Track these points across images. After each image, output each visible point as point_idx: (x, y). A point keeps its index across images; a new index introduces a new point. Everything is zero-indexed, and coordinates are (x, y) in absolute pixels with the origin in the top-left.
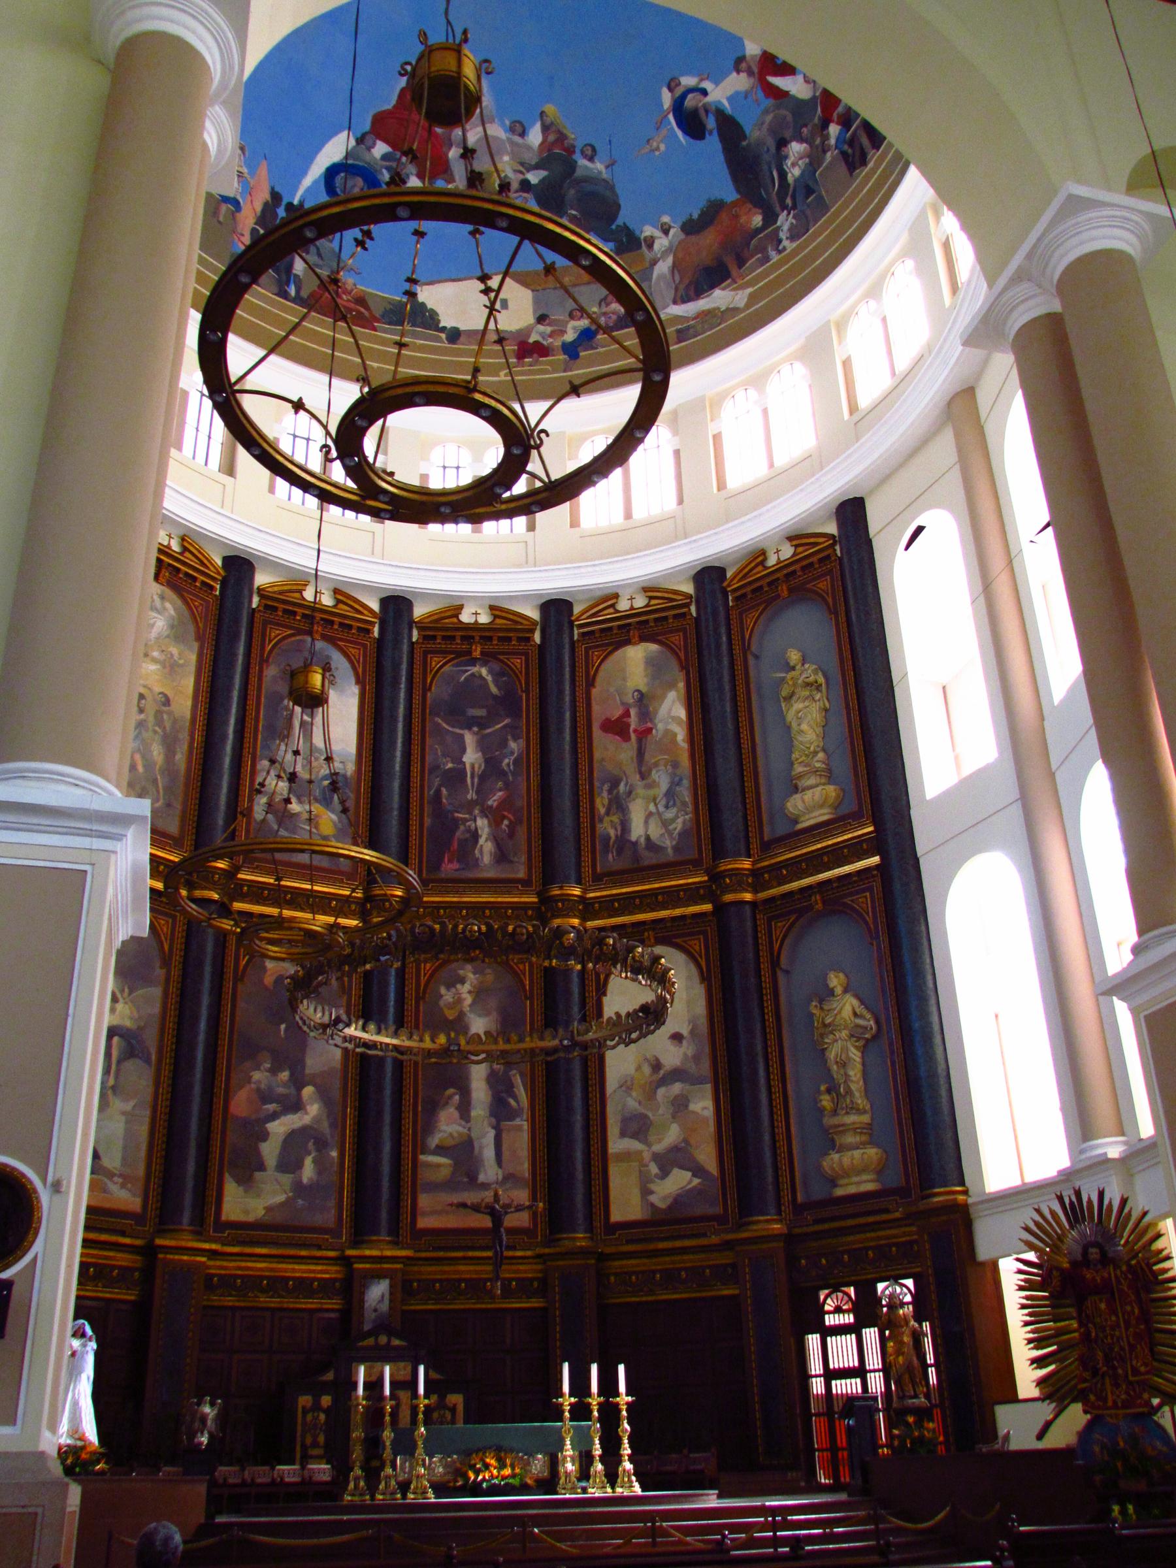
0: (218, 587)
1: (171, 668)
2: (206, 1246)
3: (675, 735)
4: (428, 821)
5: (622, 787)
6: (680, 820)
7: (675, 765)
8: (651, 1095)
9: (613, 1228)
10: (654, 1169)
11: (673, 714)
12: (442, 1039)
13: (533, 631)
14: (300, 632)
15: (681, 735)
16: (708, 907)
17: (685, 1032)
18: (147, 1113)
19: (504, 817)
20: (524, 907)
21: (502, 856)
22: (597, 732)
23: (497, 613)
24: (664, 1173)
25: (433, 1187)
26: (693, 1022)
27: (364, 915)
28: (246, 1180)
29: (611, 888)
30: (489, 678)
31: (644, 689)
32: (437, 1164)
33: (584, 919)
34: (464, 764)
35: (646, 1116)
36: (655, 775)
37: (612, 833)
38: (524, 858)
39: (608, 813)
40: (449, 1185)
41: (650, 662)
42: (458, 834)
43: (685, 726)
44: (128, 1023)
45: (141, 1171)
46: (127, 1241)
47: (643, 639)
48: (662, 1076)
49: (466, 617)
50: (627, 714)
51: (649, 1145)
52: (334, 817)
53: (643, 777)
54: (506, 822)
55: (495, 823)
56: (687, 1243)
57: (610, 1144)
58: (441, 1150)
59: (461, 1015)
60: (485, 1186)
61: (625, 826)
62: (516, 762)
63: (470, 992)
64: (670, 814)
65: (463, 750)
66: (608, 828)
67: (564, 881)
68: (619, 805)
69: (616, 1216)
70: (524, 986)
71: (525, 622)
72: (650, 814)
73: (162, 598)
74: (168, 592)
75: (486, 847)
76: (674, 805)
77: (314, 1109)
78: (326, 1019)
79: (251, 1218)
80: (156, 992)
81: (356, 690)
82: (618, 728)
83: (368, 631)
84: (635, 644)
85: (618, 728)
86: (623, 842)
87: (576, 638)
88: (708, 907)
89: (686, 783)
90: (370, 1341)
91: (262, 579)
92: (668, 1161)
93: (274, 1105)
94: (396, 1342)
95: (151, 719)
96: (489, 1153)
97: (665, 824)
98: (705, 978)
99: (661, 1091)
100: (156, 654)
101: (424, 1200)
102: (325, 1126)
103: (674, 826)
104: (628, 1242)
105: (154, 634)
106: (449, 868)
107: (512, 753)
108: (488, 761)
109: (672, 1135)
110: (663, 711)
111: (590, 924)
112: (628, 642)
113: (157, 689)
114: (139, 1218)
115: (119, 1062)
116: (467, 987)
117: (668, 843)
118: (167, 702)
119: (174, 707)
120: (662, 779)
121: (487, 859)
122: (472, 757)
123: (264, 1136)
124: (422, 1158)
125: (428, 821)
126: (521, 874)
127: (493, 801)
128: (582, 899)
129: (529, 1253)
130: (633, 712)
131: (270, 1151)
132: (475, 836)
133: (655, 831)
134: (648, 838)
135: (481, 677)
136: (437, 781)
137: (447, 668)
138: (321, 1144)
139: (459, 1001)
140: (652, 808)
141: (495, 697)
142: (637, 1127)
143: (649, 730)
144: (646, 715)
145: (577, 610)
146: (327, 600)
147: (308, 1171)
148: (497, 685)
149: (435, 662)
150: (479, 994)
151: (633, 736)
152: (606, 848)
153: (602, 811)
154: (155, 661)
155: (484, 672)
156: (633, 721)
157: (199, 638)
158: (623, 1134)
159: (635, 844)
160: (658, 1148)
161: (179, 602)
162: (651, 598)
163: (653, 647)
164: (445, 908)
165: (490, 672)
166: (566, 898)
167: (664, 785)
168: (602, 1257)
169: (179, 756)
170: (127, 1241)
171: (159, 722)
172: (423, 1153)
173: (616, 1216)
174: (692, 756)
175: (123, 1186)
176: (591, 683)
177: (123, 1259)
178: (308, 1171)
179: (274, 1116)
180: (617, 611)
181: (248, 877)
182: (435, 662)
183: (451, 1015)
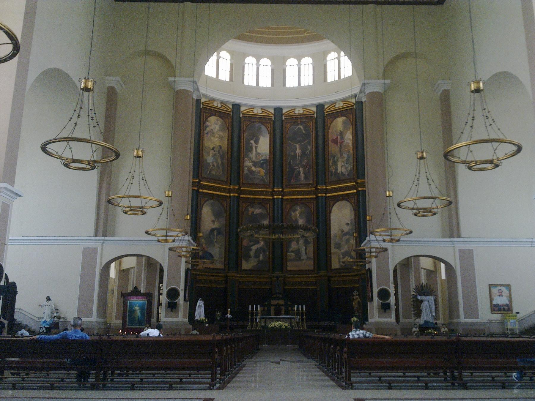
0: (231, 113)
1: (221, 138)
2: (238, 275)
3: (349, 143)
4: (287, 170)
5: (336, 158)
6: (350, 167)
7: (349, 152)
8: (341, 238)
9: (332, 270)
10: (341, 256)
11: (349, 137)
12: (277, 236)
13: (313, 114)
14: (253, 122)
15: (351, 144)
16: (355, 191)
17: (349, 223)
19: (306, 167)
20: (312, 191)
21: (306, 178)
22: (330, 142)
23: (304, 110)
24: (344, 257)
25: (291, 260)
26: (351, 220)
29: (332, 186)
30: (303, 129)
31: (342, 130)
32: (291, 255)
33: (326, 194)
34: (296, 153)
35: (340, 243)
36: (344, 155)
37: (333, 170)
38: (312, 178)
39: (332, 165)
41: (344, 122)
42: (295, 172)
43: (352, 141)
44: (218, 227)
46: (221, 275)
47: (342, 116)
48: (344, 234)
49: (297, 112)
50: (337, 138)
51: (340, 250)
52: (264, 170)
53: (341, 155)
54: (307, 168)
55: (304, 169)
56: (348, 274)
57: (332, 250)
58: (292, 252)
59: (297, 218)
60: (303, 260)
61: (336, 169)
63: (298, 213)
64: (347, 166)
65: (296, 150)
66: (332, 169)
68: (335, 163)
69: (333, 267)
70: (311, 210)
71: (312, 112)
72: (343, 166)
73: (217, 120)
74: (219, 118)
75: (302, 175)
76: (348, 163)
77: (262, 243)
78: (250, 234)
79: (248, 269)
80: (223, 219)
81: (268, 136)
82: (335, 141)
83: (271, 119)
84: (340, 117)
85: (335, 141)
86: (336, 173)
87: (325, 115)
88: (355, 191)
89: (351, 157)
90: (275, 296)
91: (242, 109)
92: (345, 254)
93: (252, 243)
94: (281, 296)
96: (304, 252)
97: (346, 168)
98: (354, 209)
99: (344, 237)
100: (217, 136)
103: (348, 169)
104: (335, 273)
105: (216, 129)
106: (293, 181)
107: (309, 149)
108: (302, 152)
109: (345, 248)
110: (346, 137)
111: (327, 195)
112: (338, 117)
113: (218, 144)
114: (224, 270)
115: (217, 236)
116: (298, 212)
117: (346, 173)
118: (221, 147)
119: (223, 148)
120: (345, 156)
121: (302, 179)
122: (298, 151)
123: (251, 250)
124: (288, 254)
125: (287, 170)
126: (311, 182)
127: (304, 163)
128: (326, 188)
129: (312, 276)
130: (339, 137)
131: (252, 253)
132: (299, 172)
133: (344, 170)
134: (342, 172)
135: (301, 129)
136: (290, 158)
137: (292, 127)
138: (264, 251)
139: (296, 215)
140: (343, 164)
142: (338, 246)
143: (343, 142)
144: (342, 138)
145: (326, 107)
146: (260, 112)
147: (261, 257)
148: (304, 131)
149: (288, 125)
150: (301, 213)
151: (339, 144)
152: (332, 175)
153: (331, 165)
154: (217, 137)
155: (301, 127)
156: (339, 139)
157: (228, 129)
158: (335, 248)
159: (339, 174)
160: (343, 251)
162: (344, 104)
163: (344, 118)
164: (292, 192)
167: (346, 158)
168: (329, 277)
170: (221, 275)
171: (219, 152)
172: (288, 252)
173: (333, 267)
174: (353, 149)
175: (219, 263)
176: (329, 129)
177: (221, 279)
178: (261, 257)
179: (253, 245)
180: (336, 108)
181: (244, 189)
182: (288, 125)
183: (294, 219)
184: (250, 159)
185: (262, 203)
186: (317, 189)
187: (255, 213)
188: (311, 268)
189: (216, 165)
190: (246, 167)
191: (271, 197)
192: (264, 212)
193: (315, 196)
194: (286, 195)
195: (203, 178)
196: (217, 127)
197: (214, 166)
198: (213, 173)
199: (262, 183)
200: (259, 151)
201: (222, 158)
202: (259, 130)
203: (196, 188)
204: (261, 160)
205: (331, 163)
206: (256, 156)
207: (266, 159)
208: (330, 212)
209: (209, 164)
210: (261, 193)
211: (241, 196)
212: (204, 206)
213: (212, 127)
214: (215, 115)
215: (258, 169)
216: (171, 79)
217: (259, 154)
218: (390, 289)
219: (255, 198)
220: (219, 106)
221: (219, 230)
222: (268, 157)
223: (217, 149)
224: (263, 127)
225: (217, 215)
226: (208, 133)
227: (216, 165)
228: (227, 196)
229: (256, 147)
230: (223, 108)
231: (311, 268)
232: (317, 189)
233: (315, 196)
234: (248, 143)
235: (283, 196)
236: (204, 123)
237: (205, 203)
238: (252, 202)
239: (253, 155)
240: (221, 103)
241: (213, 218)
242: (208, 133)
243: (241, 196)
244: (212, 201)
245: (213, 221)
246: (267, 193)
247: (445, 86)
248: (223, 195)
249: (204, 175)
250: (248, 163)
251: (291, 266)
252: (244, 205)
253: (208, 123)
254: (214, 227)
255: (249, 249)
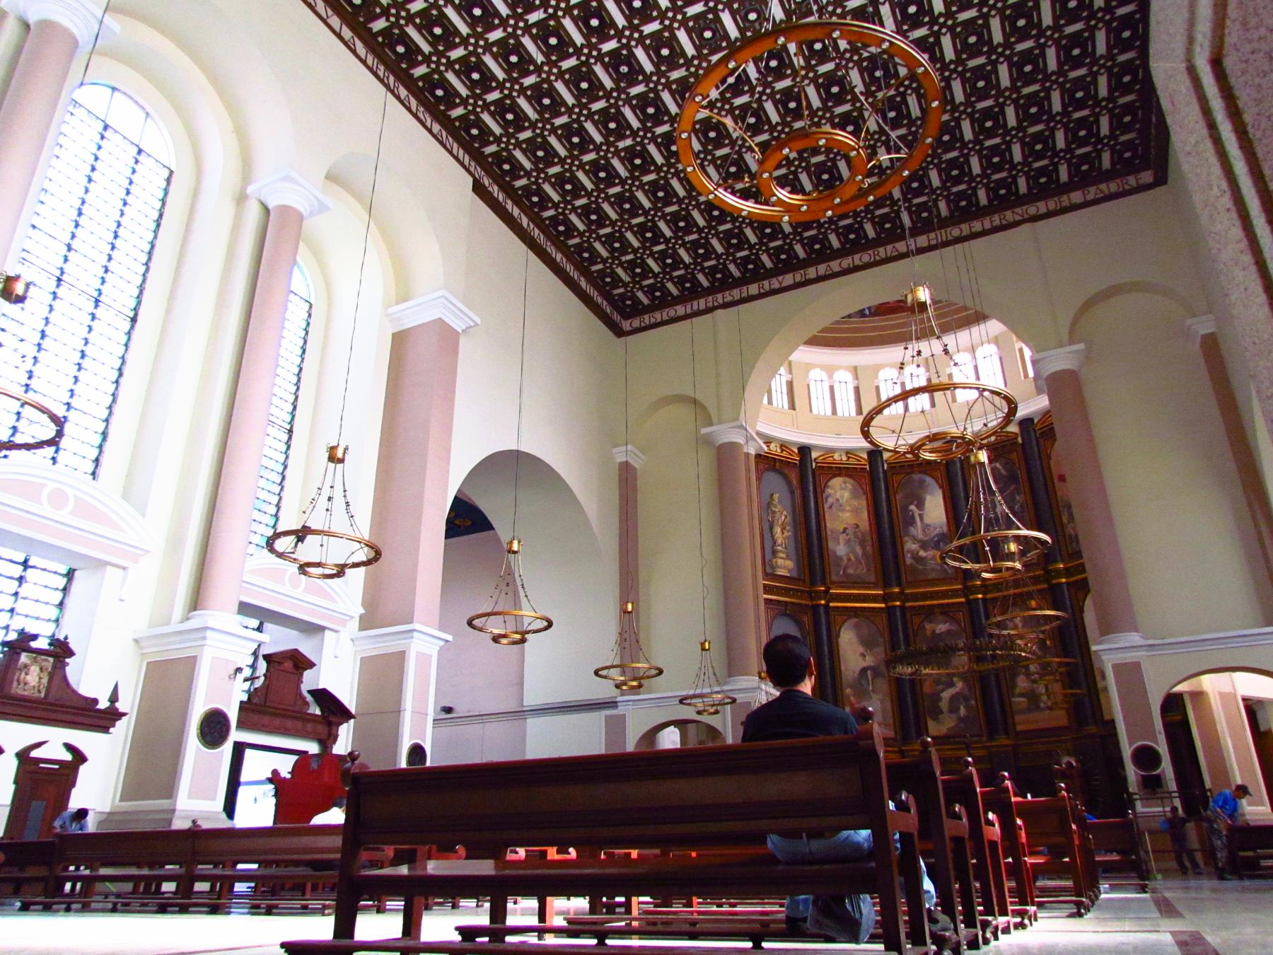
1: (855, 511)
13: (1016, 438)
14: (908, 474)
18: (888, 699)
20: (1039, 576)
25: (1020, 712)
27: (966, 596)
28: (935, 718)
32: (1020, 702)
39: (1069, 522)
40: (1029, 710)
44: (872, 664)
45: (891, 721)
58: (1021, 695)
62: (1021, 507)
67: (1056, 561)
73: (845, 482)
74: (847, 479)
77: (959, 685)
95: (853, 538)
101: (1017, 718)
102: (966, 692)
105: (845, 499)
118: (857, 526)
123: (940, 699)
124: (1013, 699)
131: (944, 705)
138: (966, 699)
141: (1004, 476)
145: (1036, 421)
147: (962, 711)
152: (1071, 543)
157: (865, 493)
161: (852, 481)
165: (1001, 464)
166: (1058, 570)
169: (868, 548)
171: (856, 536)
176: (1049, 458)
178: (962, 711)
179: (943, 690)
184: (914, 539)
185: (946, 611)
186: (1047, 572)
187: (938, 632)
188: (1064, 722)
189: (853, 558)
190: (908, 552)
191: (963, 600)
192: (954, 627)
193: (1046, 586)
194: (992, 592)
195: (833, 583)
196: (847, 495)
197: (849, 560)
198: (850, 571)
199: (942, 577)
200: (927, 520)
201: (862, 544)
202: (922, 482)
203: (823, 602)
204: (937, 535)
205: (1065, 519)
206: (924, 530)
207: (943, 534)
208: (1082, 611)
209: (840, 558)
210: (945, 594)
211: (908, 604)
212: (842, 630)
213: (838, 495)
214: (839, 475)
215: (931, 553)
216: (704, 431)
217: (928, 526)
218: (1157, 744)
219: (933, 605)
220: (844, 458)
221: (874, 669)
222: (945, 529)
223: (850, 531)
224: (929, 480)
225: (867, 643)
226: (831, 507)
227: (853, 558)
228: (882, 608)
229: (921, 516)
230: (851, 461)
231: (1064, 722)
232: (1047, 572)
233: (1046, 586)
234: (905, 508)
235: (984, 593)
236: (823, 491)
237: (843, 623)
238: (929, 613)
239: (917, 531)
240: (847, 453)
241: (861, 649)
242: (831, 507)
243: (908, 604)
244: (855, 620)
245: (863, 655)
246: (955, 593)
247: (1204, 326)
248: (874, 608)
249: (834, 578)
250: (910, 546)
251: (1023, 723)
252: (916, 620)
253: (829, 491)
254: (865, 664)
255: (936, 697)
